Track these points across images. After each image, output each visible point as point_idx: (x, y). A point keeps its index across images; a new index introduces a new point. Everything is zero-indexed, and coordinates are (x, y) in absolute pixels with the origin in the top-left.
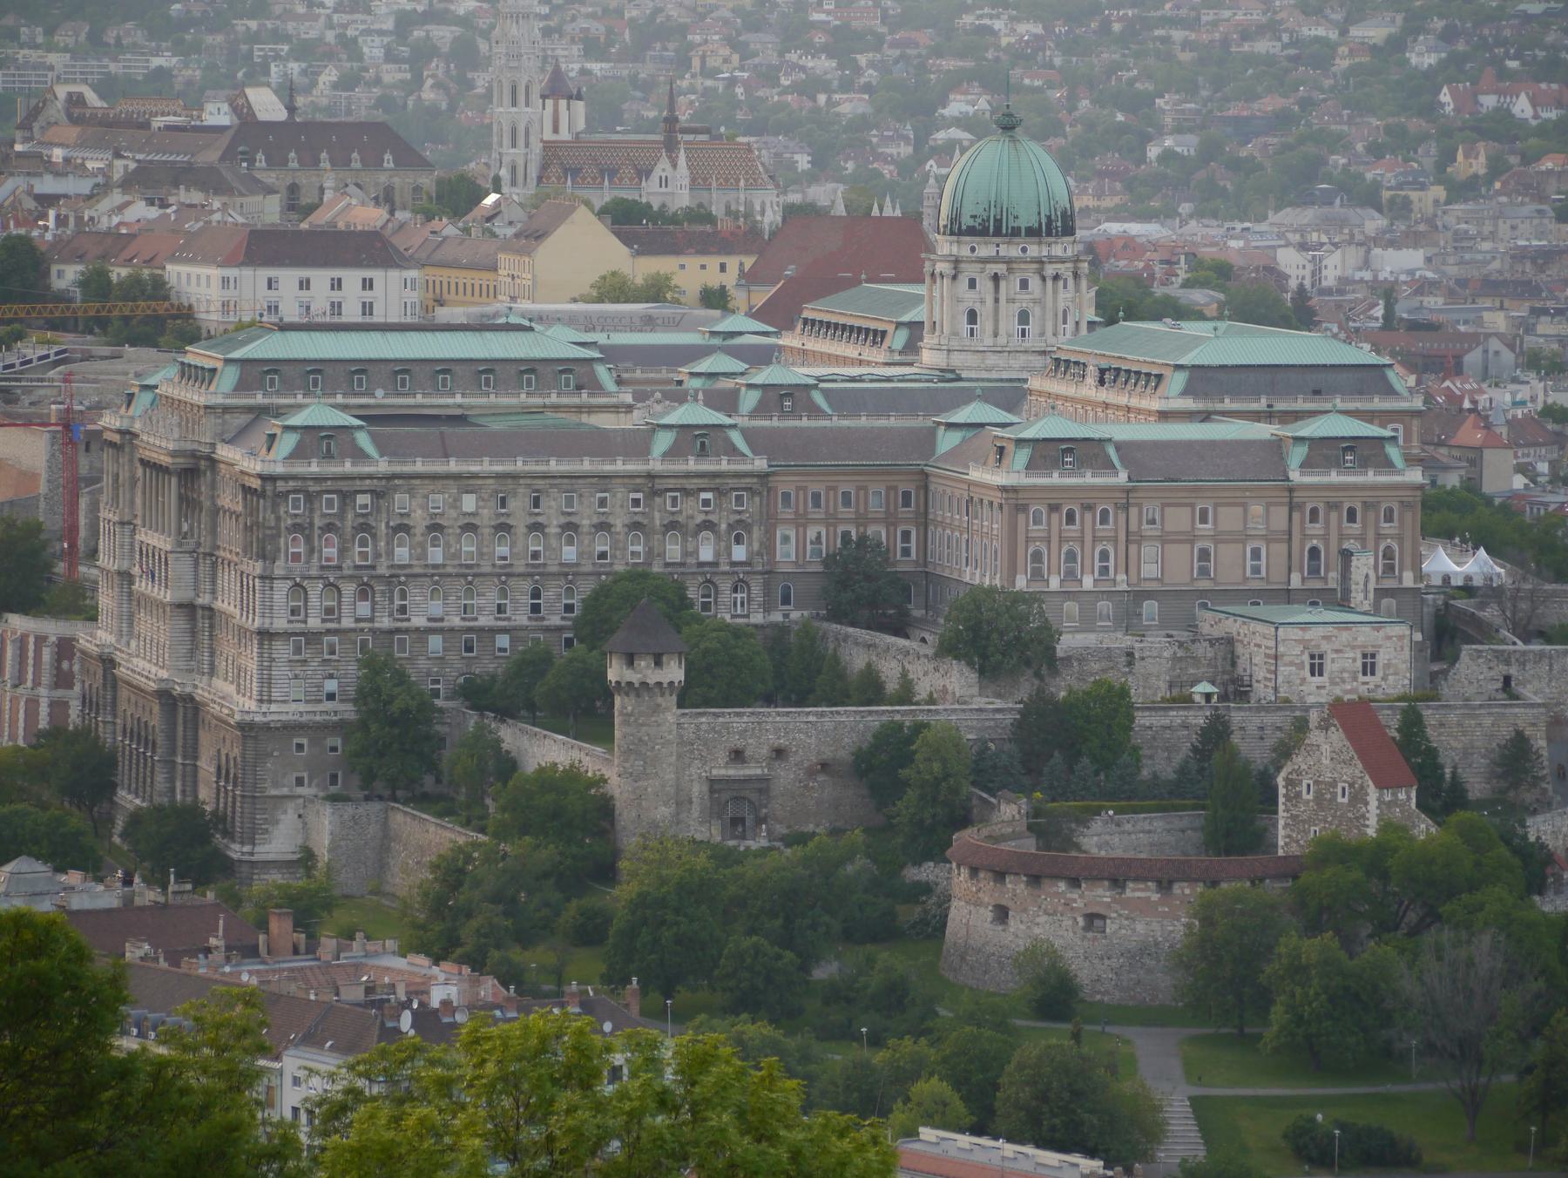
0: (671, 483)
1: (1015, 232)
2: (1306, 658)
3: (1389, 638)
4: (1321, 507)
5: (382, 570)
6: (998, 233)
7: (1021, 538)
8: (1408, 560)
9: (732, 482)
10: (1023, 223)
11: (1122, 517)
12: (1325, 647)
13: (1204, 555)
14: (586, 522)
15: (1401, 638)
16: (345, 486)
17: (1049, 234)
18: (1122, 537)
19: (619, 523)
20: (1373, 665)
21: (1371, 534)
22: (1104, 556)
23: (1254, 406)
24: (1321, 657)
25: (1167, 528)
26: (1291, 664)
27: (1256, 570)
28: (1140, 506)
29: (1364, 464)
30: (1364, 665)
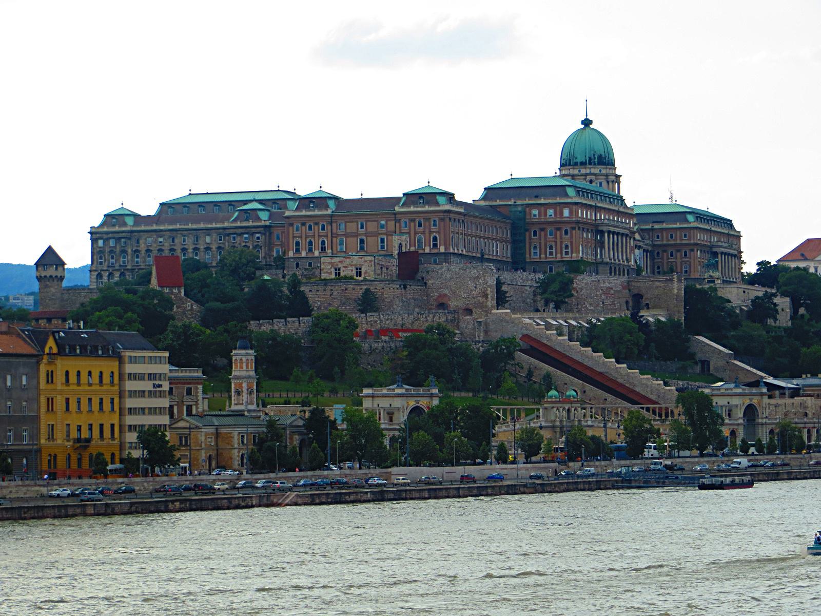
0: (232, 231)
1: (576, 164)
2: (333, 270)
3: (366, 261)
4: (407, 221)
5: (129, 267)
6: (570, 165)
7: (291, 236)
8: (442, 242)
9: (254, 230)
10: (579, 160)
11: (329, 228)
12: (340, 265)
13: (362, 241)
14: (202, 247)
15: (371, 261)
16: (116, 236)
17: (590, 164)
18: (330, 235)
19: (214, 247)
20: (360, 272)
21: (427, 231)
22: (323, 242)
23: (509, 203)
24: (339, 270)
25: (348, 231)
26: (327, 272)
27: (382, 247)
28: (336, 222)
29: (428, 203)
30: (357, 272)
